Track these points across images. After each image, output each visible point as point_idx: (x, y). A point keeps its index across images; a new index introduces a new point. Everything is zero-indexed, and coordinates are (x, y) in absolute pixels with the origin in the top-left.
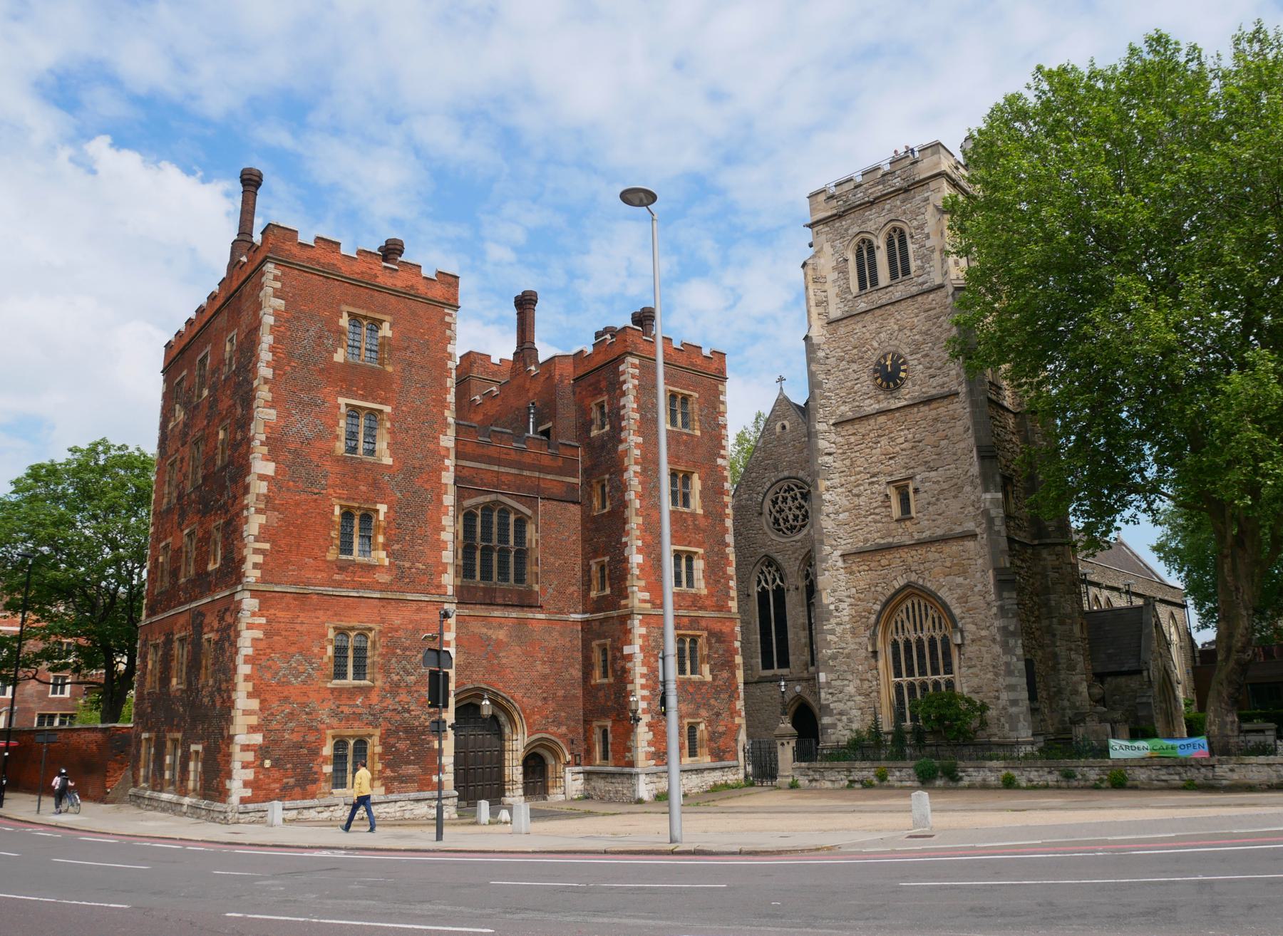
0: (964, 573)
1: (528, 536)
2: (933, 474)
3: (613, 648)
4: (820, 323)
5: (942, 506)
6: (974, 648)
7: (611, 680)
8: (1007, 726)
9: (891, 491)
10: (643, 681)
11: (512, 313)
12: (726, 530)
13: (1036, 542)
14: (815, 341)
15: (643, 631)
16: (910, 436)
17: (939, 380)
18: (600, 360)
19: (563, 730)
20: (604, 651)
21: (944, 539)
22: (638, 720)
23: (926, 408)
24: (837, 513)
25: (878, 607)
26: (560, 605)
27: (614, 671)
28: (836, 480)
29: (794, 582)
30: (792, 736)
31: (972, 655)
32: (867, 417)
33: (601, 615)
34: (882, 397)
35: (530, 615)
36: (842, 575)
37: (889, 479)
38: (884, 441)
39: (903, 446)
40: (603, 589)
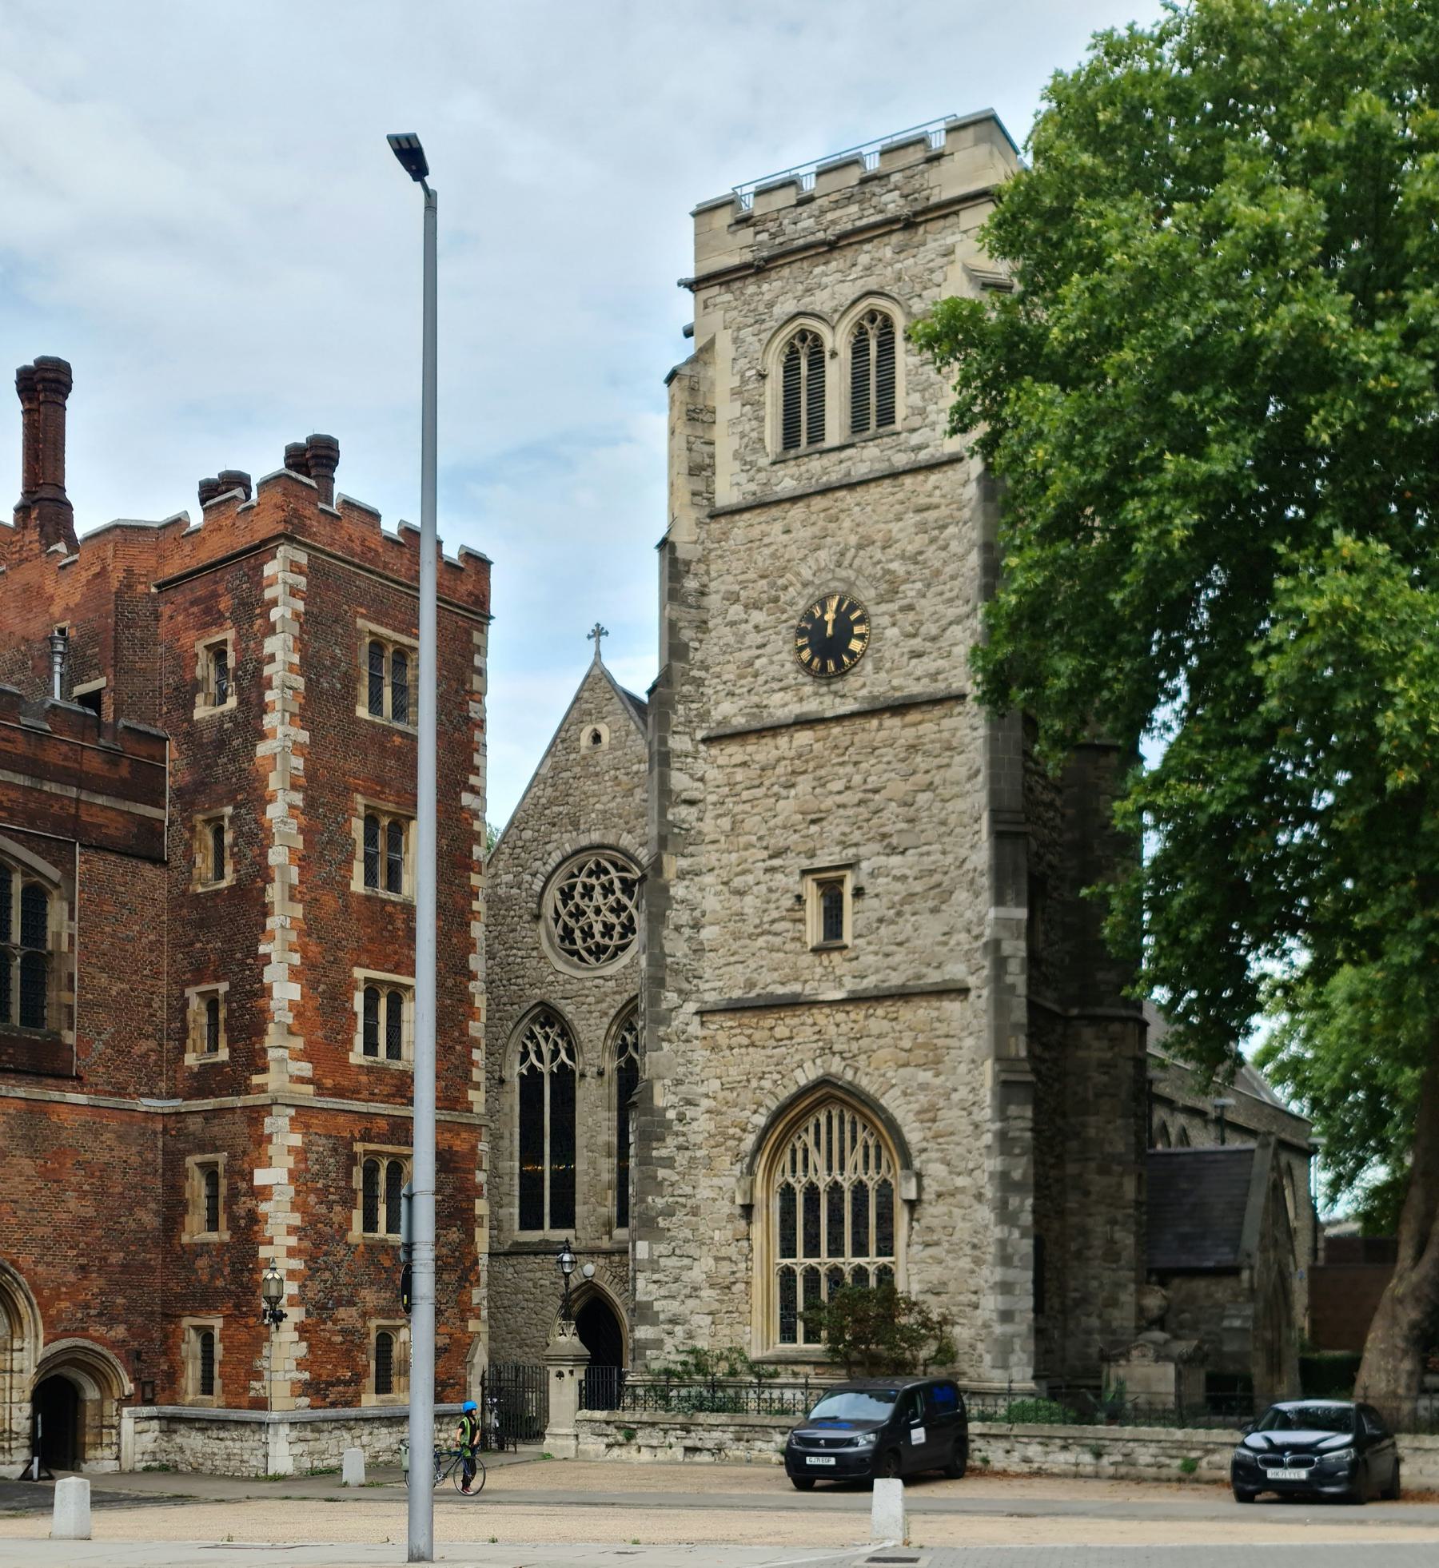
0: (935, 1063)
1: (52, 925)
2: (895, 860)
3: (231, 1172)
4: (694, 514)
5: (905, 927)
6: (940, 1209)
7: (224, 1235)
8: (988, 1358)
9: (811, 890)
10: (293, 1241)
11: (13, 410)
12: (471, 946)
13: (1074, 1012)
14: (681, 554)
15: (297, 1140)
16: (857, 779)
17: (928, 664)
18: (216, 548)
19: (120, 1332)
20: (211, 1173)
21: (903, 995)
22: (279, 1317)
23: (896, 722)
24: (697, 926)
25: (761, 1120)
26: (120, 1077)
27: (233, 1219)
28: (707, 856)
29: (596, 1058)
30: (578, 1359)
31: (935, 1223)
32: (774, 730)
33: (210, 1103)
34: (808, 690)
35: (55, 1095)
36: (700, 1054)
37: (806, 864)
38: (804, 784)
39: (839, 799)
40: (214, 1047)
